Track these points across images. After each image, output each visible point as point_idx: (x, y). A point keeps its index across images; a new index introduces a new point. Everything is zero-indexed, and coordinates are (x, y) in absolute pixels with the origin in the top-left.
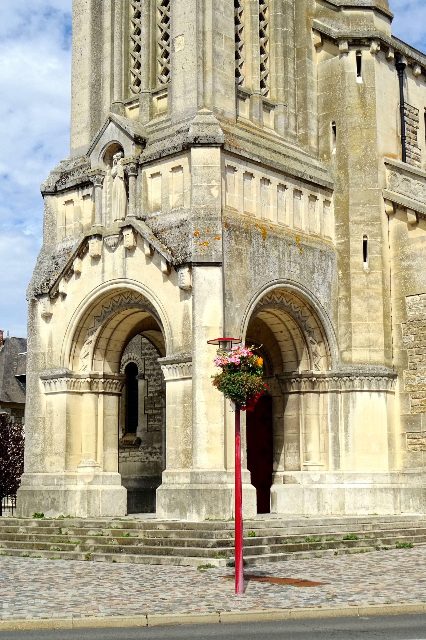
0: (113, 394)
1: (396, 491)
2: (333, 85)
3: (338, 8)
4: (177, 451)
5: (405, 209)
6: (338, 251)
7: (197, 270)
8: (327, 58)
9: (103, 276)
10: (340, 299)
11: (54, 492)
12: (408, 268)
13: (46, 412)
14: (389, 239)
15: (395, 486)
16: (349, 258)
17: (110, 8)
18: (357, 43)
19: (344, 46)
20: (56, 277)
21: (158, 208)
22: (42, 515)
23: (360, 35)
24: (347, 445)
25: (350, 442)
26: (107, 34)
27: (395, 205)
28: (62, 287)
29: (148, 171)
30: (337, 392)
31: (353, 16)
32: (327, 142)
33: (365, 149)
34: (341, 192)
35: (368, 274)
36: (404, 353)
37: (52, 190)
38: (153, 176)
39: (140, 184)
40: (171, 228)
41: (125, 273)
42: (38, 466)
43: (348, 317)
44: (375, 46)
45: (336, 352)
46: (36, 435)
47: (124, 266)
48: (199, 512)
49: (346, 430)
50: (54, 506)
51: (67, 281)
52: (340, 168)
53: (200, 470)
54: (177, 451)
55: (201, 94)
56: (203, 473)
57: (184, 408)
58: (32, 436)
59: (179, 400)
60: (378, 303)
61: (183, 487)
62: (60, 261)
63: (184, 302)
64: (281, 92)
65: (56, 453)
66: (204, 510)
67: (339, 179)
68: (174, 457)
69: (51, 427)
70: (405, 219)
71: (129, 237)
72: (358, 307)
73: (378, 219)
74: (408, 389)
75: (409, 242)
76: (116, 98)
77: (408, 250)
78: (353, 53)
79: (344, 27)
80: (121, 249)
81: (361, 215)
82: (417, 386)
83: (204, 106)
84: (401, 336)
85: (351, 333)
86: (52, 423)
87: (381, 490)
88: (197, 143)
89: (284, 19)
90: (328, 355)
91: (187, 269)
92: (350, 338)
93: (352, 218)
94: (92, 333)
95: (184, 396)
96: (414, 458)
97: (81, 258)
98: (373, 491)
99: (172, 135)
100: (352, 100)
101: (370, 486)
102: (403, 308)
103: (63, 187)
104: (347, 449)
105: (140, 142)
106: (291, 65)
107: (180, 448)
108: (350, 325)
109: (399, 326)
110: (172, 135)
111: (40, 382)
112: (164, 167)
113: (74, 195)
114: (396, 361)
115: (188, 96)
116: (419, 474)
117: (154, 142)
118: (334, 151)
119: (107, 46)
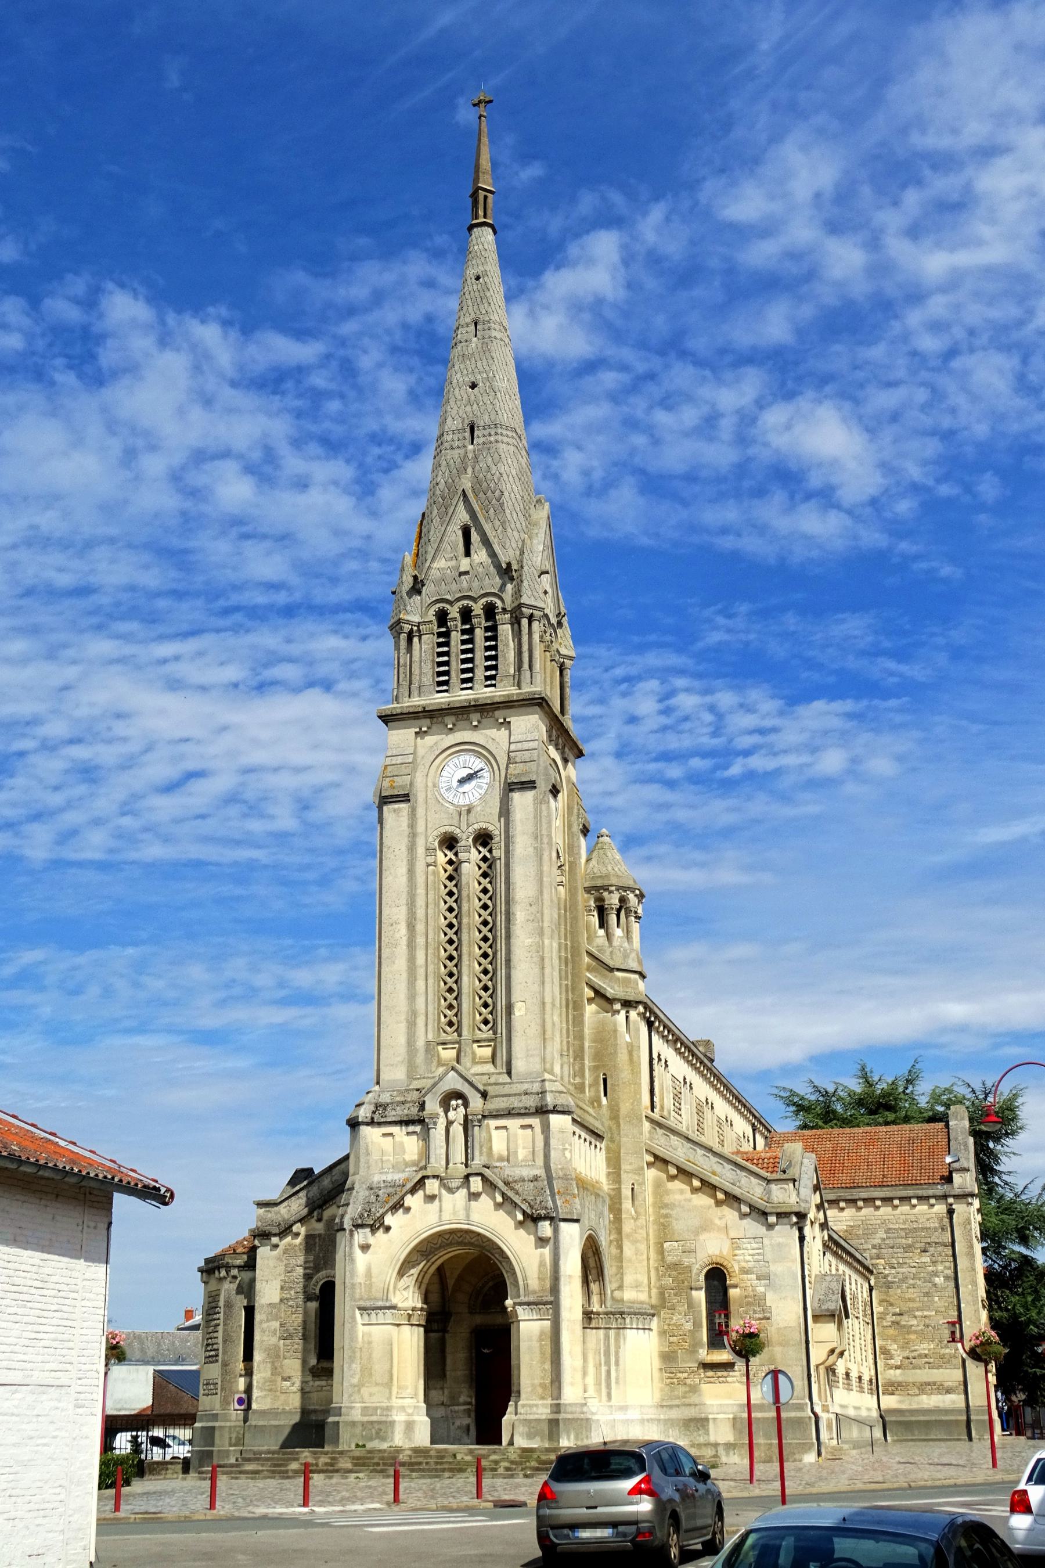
0: (418, 1325)
1: (659, 1420)
2: (605, 1039)
3: (611, 970)
4: (533, 1385)
5: (666, 1162)
6: (609, 1195)
7: (562, 1225)
8: (598, 1013)
9: (440, 1216)
10: (611, 1241)
11: (379, 1423)
12: (667, 1216)
13: (363, 1342)
14: (649, 1188)
15: (657, 1417)
16: (621, 1204)
17: (424, 947)
18: (627, 1004)
19: (617, 1006)
20: (381, 1211)
21: (501, 1159)
22: (364, 1446)
23: (631, 998)
24: (617, 1379)
25: (621, 1376)
26: (421, 972)
27: (656, 1157)
28: (389, 1220)
29: (493, 1123)
30: (610, 1328)
31: (625, 979)
32: (598, 1091)
33: (632, 1104)
34: (612, 1140)
35: (636, 1219)
36: (662, 1294)
37: (368, 1120)
38: (497, 1128)
39: (484, 1134)
40: (524, 1181)
41: (468, 1216)
42: (357, 1397)
43: (620, 1258)
44: (641, 1009)
45: (609, 1292)
46: (354, 1366)
47: (468, 1210)
48: (569, 1439)
49: (617, 1364)
50: (381, 1436)
51: (393, 1214)
52: (611, 1119)
53: (566, 1402)
54: (533, 1385)
55: (544, 1060)
56: (570, 1405)
57: (541, 1345)
58: (350, 1366)
59: (535, 1338)
60: (643, 1247)
61: (544, 1417)
62: (380, 1193)
63: (539, 1250)
64: (565, 1043)
65: (377, 1384)
66: (572, 1437)
67: (610, 1129)
68: (530, 1389)
69: (370, 1358)
70: (667, 1172)
71: (476, 1184)
72: (628, 1250)
73: (643, 1168)
74: (666, 1327)
75: (667, 1192)
76: (430, 1037)
77: (667, 1200)
78: (623, 1013)
79: (616, 988)
80: (463, 1192)
81: (631, 1164)
82: (674, 1325)
83: (545, 1070)
84: (659, 1279)
85: (622, 1274)
86: (371, 1354)
87: (648, 1420)
88: (555, 1111)
89: (567, 972)
90: (602, 1293)
91: (547, 1223)
92: (622, 1279)
93: (623, 1167)
94: (413, 1267)
95: (541, 1335)
96: (672, 1391)
97: (412, 1194)
98: (642, 1421)
99: (520, 1095)
100: (623, 1056)
101: (639, 1417)
102: (661, 1252)
103: (382, 1120)
104: (617, 1382)
105: (484, 1095)
106: (571, 1017)
107: (537, 1382)
108: (621, 1267)
109: (657, 1269)
110: (520, 1095)
111: (357, 1312)
112: (513, 1124)
113: (395, 1130)
114: (654, 1301)
115: (531, 1059)
116: (678, 1406)
117: (497, 1096)
118: (604, 1100)
119: (420, 984)
